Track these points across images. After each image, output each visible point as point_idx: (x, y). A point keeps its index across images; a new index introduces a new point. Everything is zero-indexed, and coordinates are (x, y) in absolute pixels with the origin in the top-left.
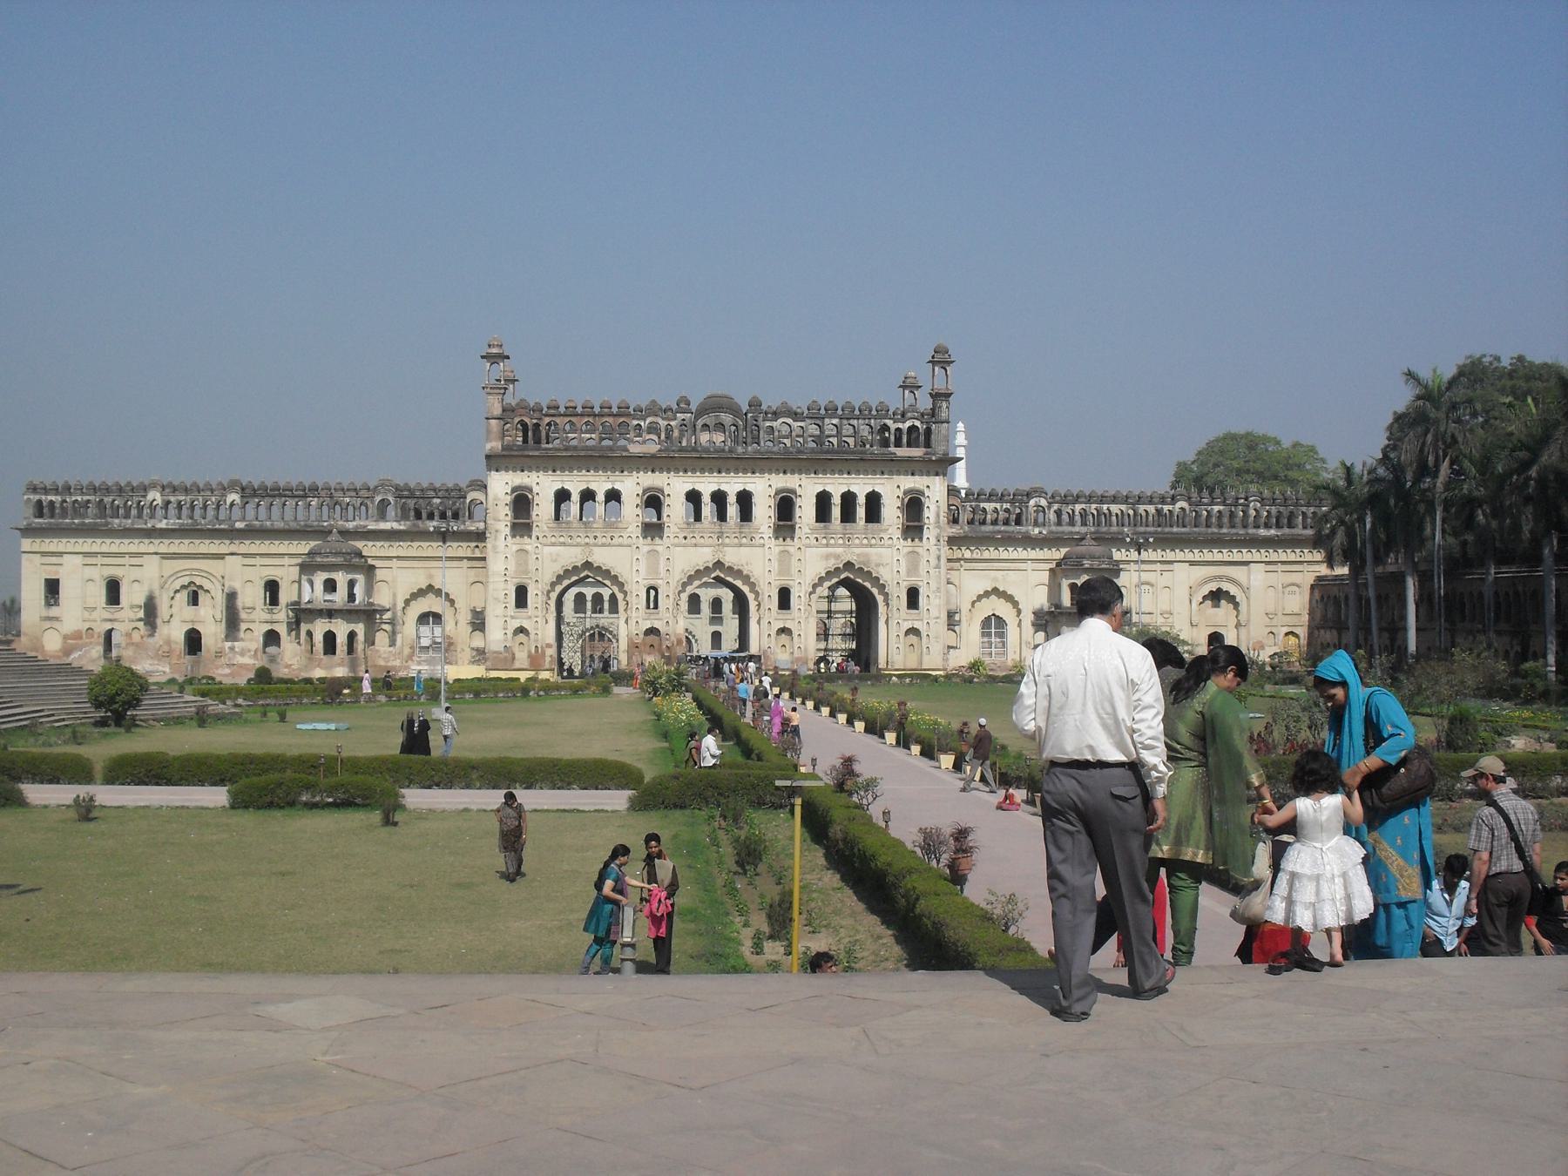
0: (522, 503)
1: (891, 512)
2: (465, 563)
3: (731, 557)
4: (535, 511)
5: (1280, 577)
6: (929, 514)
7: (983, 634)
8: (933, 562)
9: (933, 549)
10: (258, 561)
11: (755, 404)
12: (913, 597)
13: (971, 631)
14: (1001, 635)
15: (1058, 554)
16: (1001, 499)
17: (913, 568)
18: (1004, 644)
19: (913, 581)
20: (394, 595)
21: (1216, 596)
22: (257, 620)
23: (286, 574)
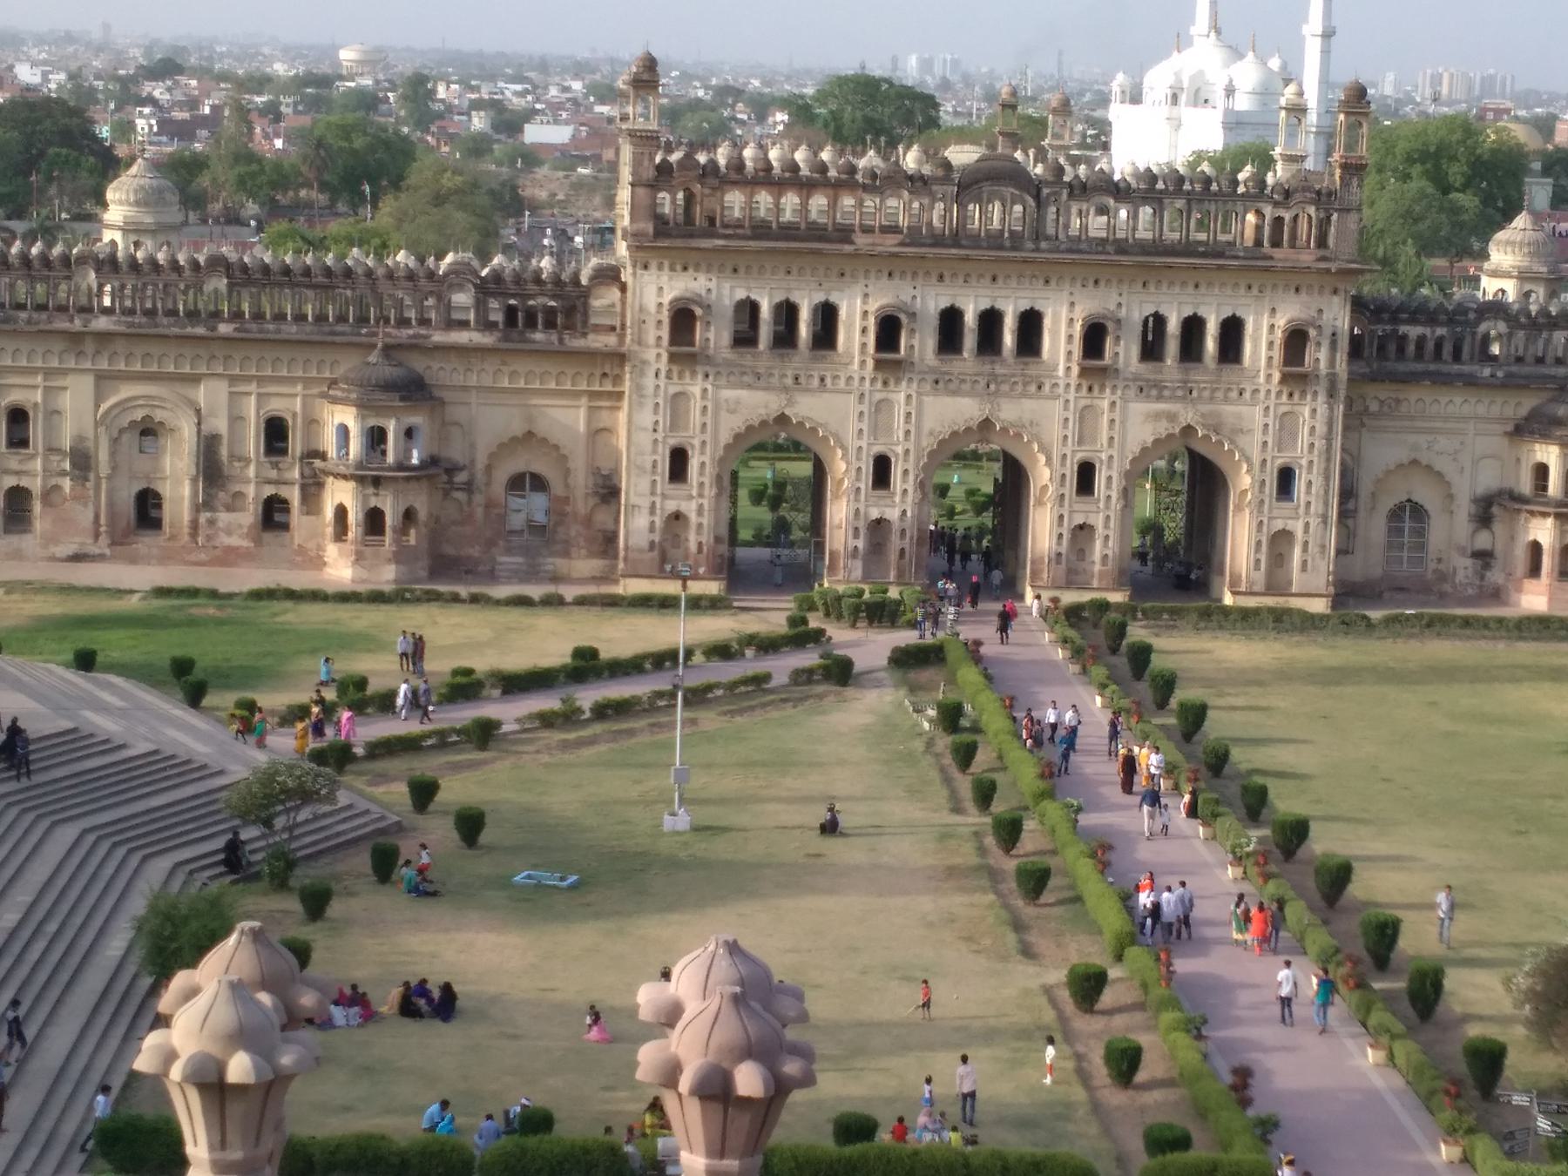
2: (584, 401)
3: (1009, 411)
6: (1318, 356)
7: (1395, 530)
8: (1321, 429)
9: (1322, 409)
10: (253, 387)
12: (1286, 478)
13: (1375, 528)
14: (1420, 533)
18: (1422, 547)
20: (472, 446)
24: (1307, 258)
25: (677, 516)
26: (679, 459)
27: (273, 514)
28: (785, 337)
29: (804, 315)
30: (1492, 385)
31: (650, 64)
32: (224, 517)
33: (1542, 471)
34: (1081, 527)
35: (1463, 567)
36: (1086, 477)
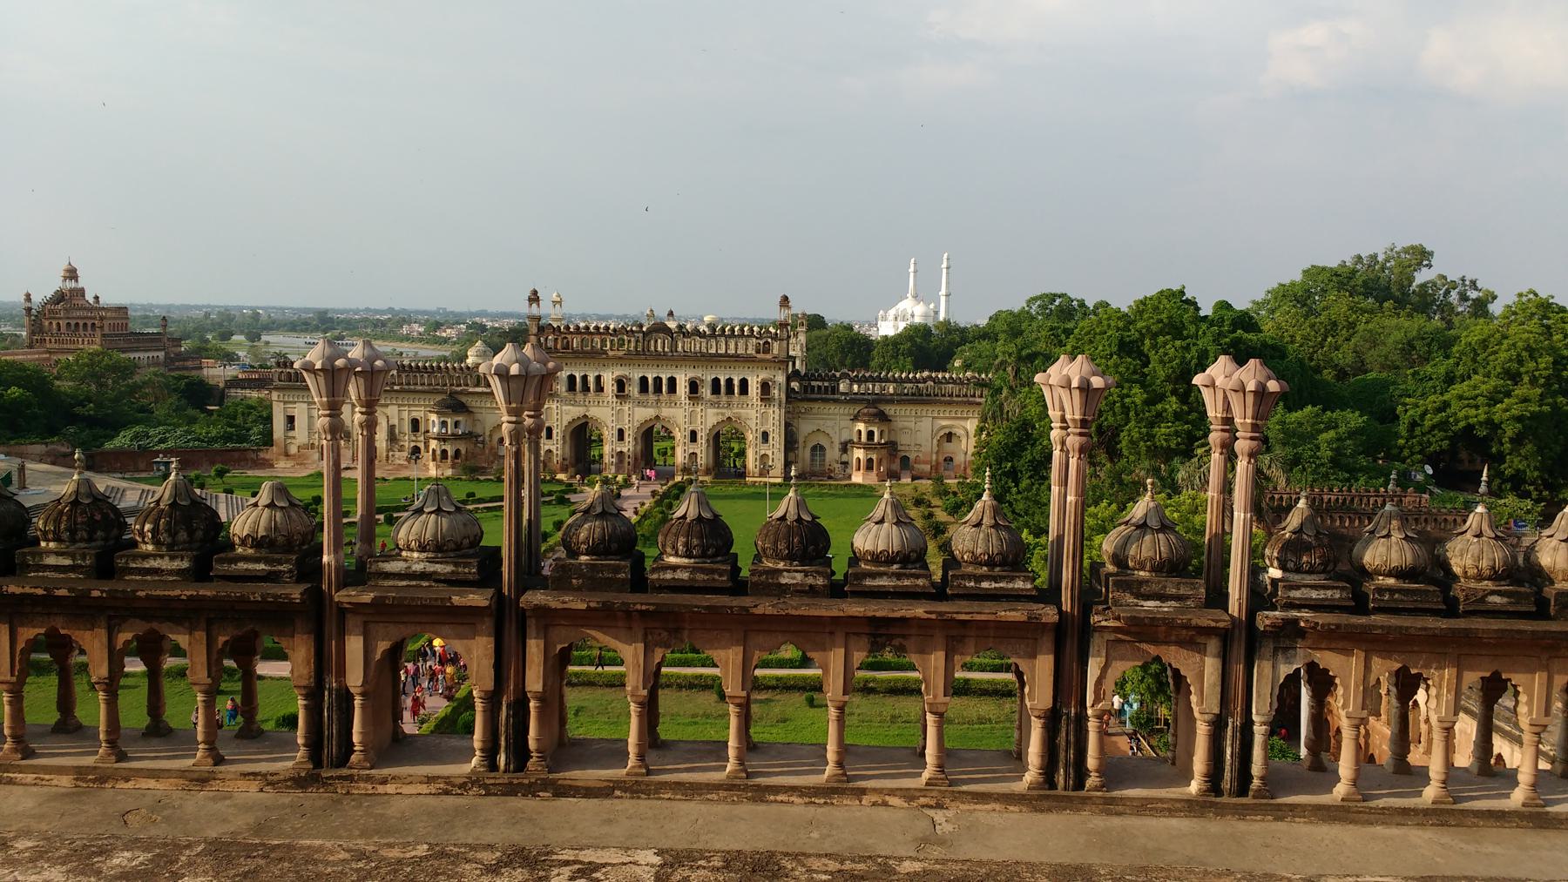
1: (754, 388)
12: (765, 436)
16: (823, 380)
22: (407, 442)
24: (768, 357)
27: (416, 450)
28: (586, 389)
30: (847, 402)
31: (535, 293)
32: (397, 454)
35: (838, 466)
36: (693, 436)
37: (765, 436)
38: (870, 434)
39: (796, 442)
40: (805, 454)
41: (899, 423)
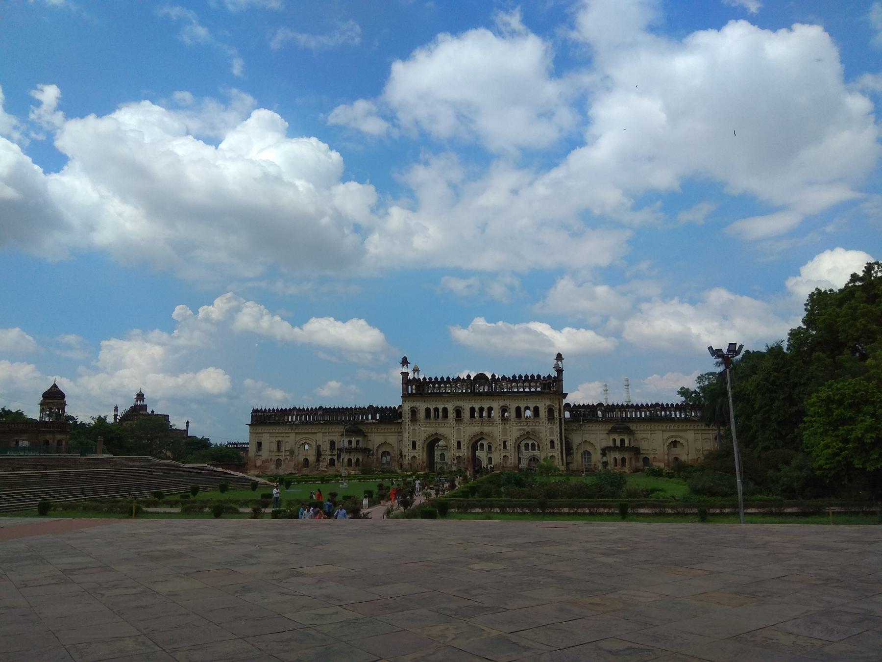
0: (414, 412)
3: (486, 429)
4: (418, 416)
5: (699, 436)
6: (556, 414)
11: (493, 376)
12: (552, 443)
14: (590, 458)
15: (609, 427)
17: (551, 433)
19: (552, 438)
21: (675, 444)
22: (327, 456)
23: (335, 438)
25: (414, 457)
26: (414, 443)
27: (332, 463)
28: (436, 417)
29: (440, 410)
33: (614, 440)
34: (505, 456)
37: (552, 443)
38: (622, 441)
39: (572, 449)
40: (578, 457)
41: (639, 435)
